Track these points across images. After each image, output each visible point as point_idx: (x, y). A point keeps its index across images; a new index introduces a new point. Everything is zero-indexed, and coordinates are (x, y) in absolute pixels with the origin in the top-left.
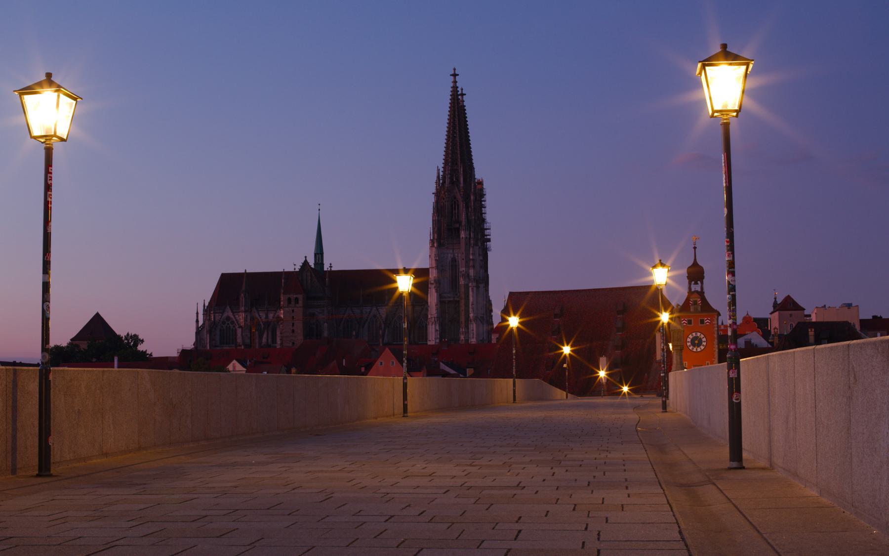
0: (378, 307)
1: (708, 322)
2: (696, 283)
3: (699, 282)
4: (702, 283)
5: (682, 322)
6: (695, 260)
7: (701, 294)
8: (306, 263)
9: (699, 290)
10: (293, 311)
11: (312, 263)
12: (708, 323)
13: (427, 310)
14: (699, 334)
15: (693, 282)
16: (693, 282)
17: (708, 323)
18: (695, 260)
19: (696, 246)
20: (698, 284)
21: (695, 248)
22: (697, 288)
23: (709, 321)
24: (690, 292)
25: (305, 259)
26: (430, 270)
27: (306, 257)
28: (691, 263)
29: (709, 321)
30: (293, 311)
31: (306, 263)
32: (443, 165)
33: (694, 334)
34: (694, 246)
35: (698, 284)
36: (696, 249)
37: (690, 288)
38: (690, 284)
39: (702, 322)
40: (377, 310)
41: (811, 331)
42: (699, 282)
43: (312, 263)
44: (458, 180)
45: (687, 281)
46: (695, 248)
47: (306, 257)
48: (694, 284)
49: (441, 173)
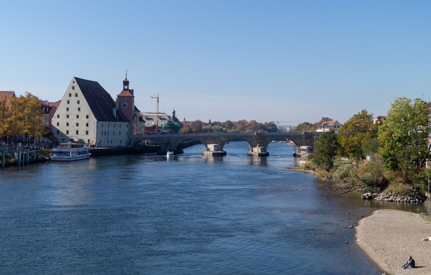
2: (126, 86)
6: (126, 78)
18: (126, 78)
21: (126, 74)
22: (126, 88)
28: (124, 79)
37: (124, 88)
38: (124, 86)
45: (123, 85)
46: (126, 74)
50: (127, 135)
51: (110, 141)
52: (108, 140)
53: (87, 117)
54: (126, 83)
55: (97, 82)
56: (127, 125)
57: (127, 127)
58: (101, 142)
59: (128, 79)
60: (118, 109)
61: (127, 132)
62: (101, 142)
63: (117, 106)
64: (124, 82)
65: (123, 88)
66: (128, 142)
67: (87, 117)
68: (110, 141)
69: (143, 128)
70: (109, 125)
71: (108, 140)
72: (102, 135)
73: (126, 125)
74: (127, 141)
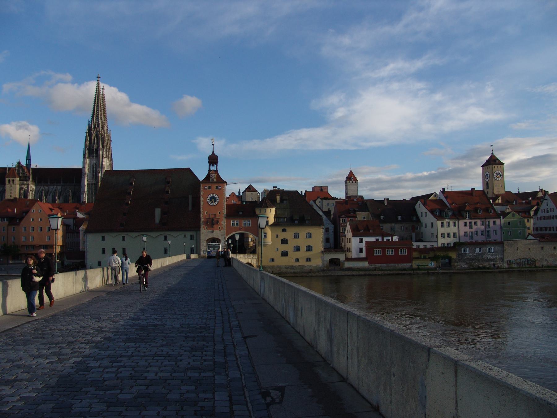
0: (57, 186)
1: (220, 188)
3: (215, 165)
4: (217, 166)
5: (205, 188)
7: (216, 171)
8: (19, 163)
10: (11, 186)
11: (24, 163)
12: (220, 189)
13: (81, 188)
14: (214, 195)
15: (212, 165)
16: (212, 165)
17: (220, 189)
19: (214, 144)
20: (214, 166)
21: (213, 145)
22: (214, 168)
23: (221, 188)
24: (210, 171)
25: (19, 161)
26: (83, 169)
27: (19, 160)
28: (211, 153)
29: (221, 188)
30: (11, 186)
31: (19, 163)
32: (91, 119)
33: (212, 195)
35: (214, 166)
37: (210, 168)
38: (210, 166)
39: (217, 188)
40: (57, 187)
41: (278, 195)
43: (24, 163)
44: (98, 126)
46: (213, 145)
47: (19, 160)
48: (212, 166)
49: (90, 123)
54: (213, 160)
55: (189, 169)
59: (216, 153)
64: (210, 158)
65: (208, 169)
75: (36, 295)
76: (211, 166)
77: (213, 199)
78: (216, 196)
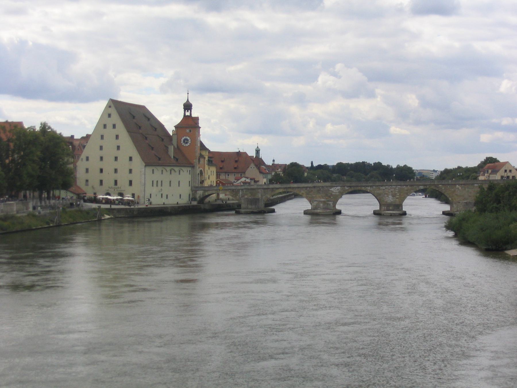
3: (189, 111)
4: (191, 112)
6: (188, 99)
9: (189, 115)
14: (187, 137)
15: (186, 111)
18: (188, 99)
19: (189, 92)
21: (188, 93)
22: (188, 114)
28: (185, 101)
34: (187, 92)
36: (189, 94)
42: (189, 111)
45: (183, 109)
46: (188, 93)
50: (189, 186)
51: (164, 196)
52: (162, 194)
53: (131, 159)
54: (188, 107)
56: (190, 171)
57: (190, 174)
58: (151, 197)
60: (176, 147)
61: (189, 182)
62: (152, 196)
63: (175, 142)
65: (183, 115)
66: (191, 197)
67: (131, 159)
68: (164, 196)
69: (213, 175)
70: (162, 170)
71: (162, 194)
72: (153, 186)
73: (189, 171)
74: (189, 195)
75: (271, 208)
76: (186, 112)
77: (186, 141)
78: (189, 138)
